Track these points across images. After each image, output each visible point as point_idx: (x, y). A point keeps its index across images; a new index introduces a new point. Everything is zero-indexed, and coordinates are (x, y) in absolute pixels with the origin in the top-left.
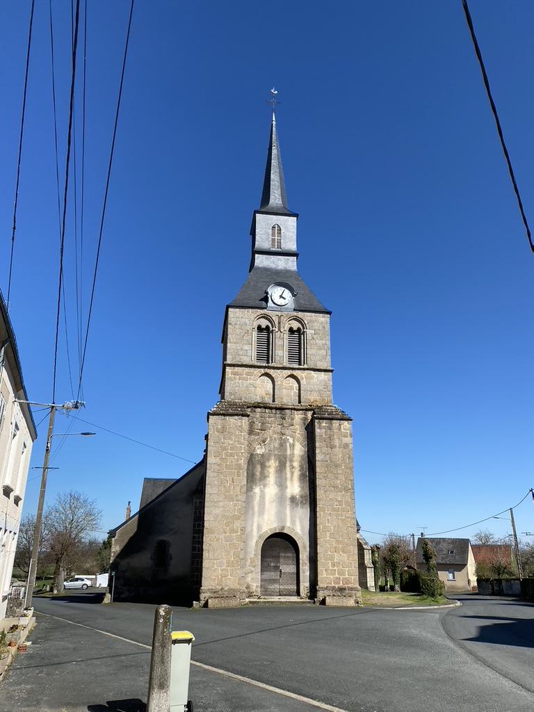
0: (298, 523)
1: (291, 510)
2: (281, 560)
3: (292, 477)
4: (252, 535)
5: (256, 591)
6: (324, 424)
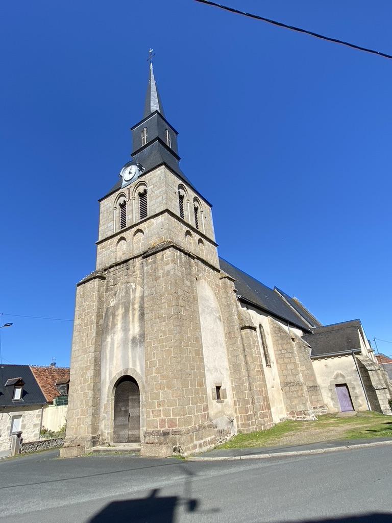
0: (138, 363)
1: (132, 351)
2: (130, 404)
3: (133, 319)
4: (105, 381)
5: (107, 438)
6: (150, 261)
